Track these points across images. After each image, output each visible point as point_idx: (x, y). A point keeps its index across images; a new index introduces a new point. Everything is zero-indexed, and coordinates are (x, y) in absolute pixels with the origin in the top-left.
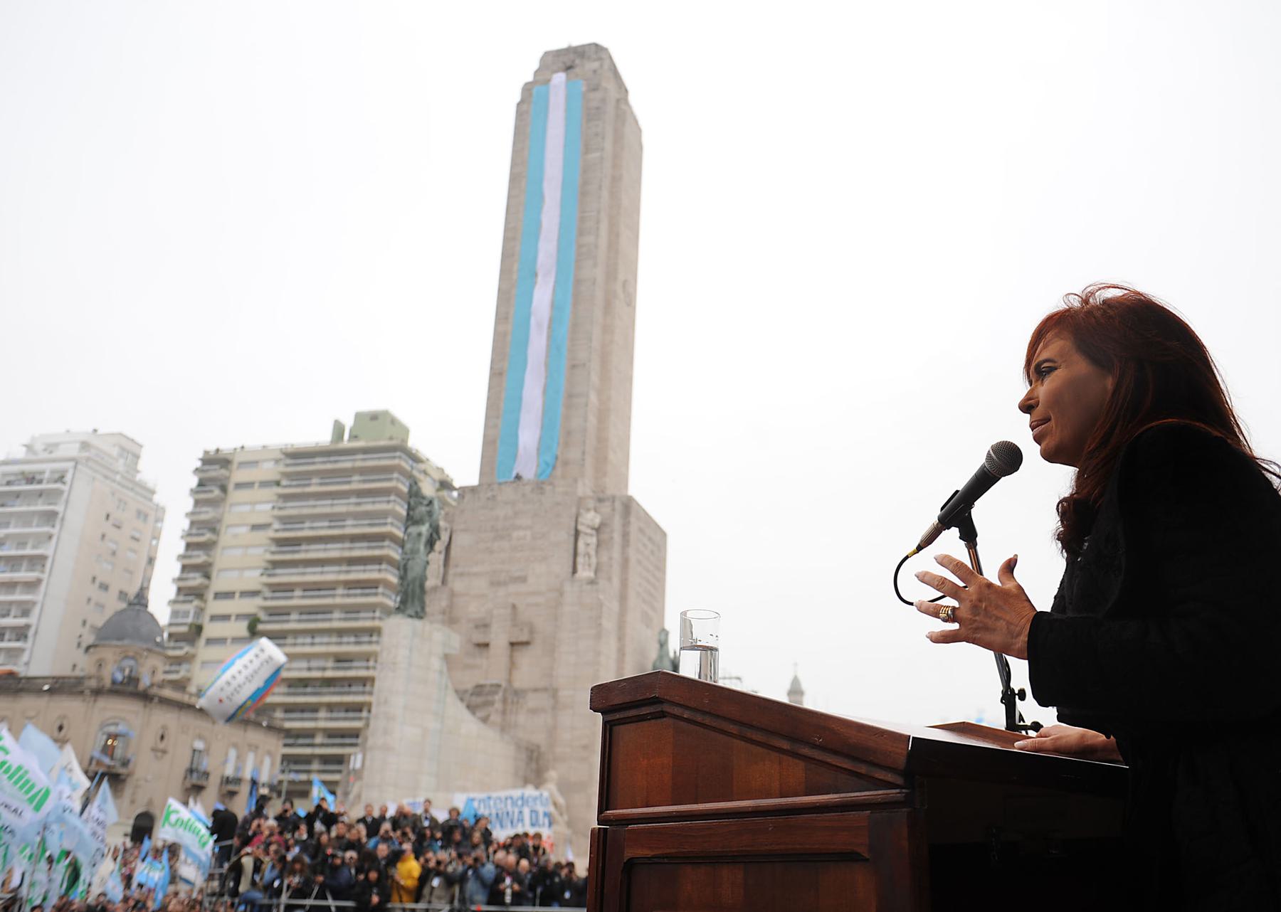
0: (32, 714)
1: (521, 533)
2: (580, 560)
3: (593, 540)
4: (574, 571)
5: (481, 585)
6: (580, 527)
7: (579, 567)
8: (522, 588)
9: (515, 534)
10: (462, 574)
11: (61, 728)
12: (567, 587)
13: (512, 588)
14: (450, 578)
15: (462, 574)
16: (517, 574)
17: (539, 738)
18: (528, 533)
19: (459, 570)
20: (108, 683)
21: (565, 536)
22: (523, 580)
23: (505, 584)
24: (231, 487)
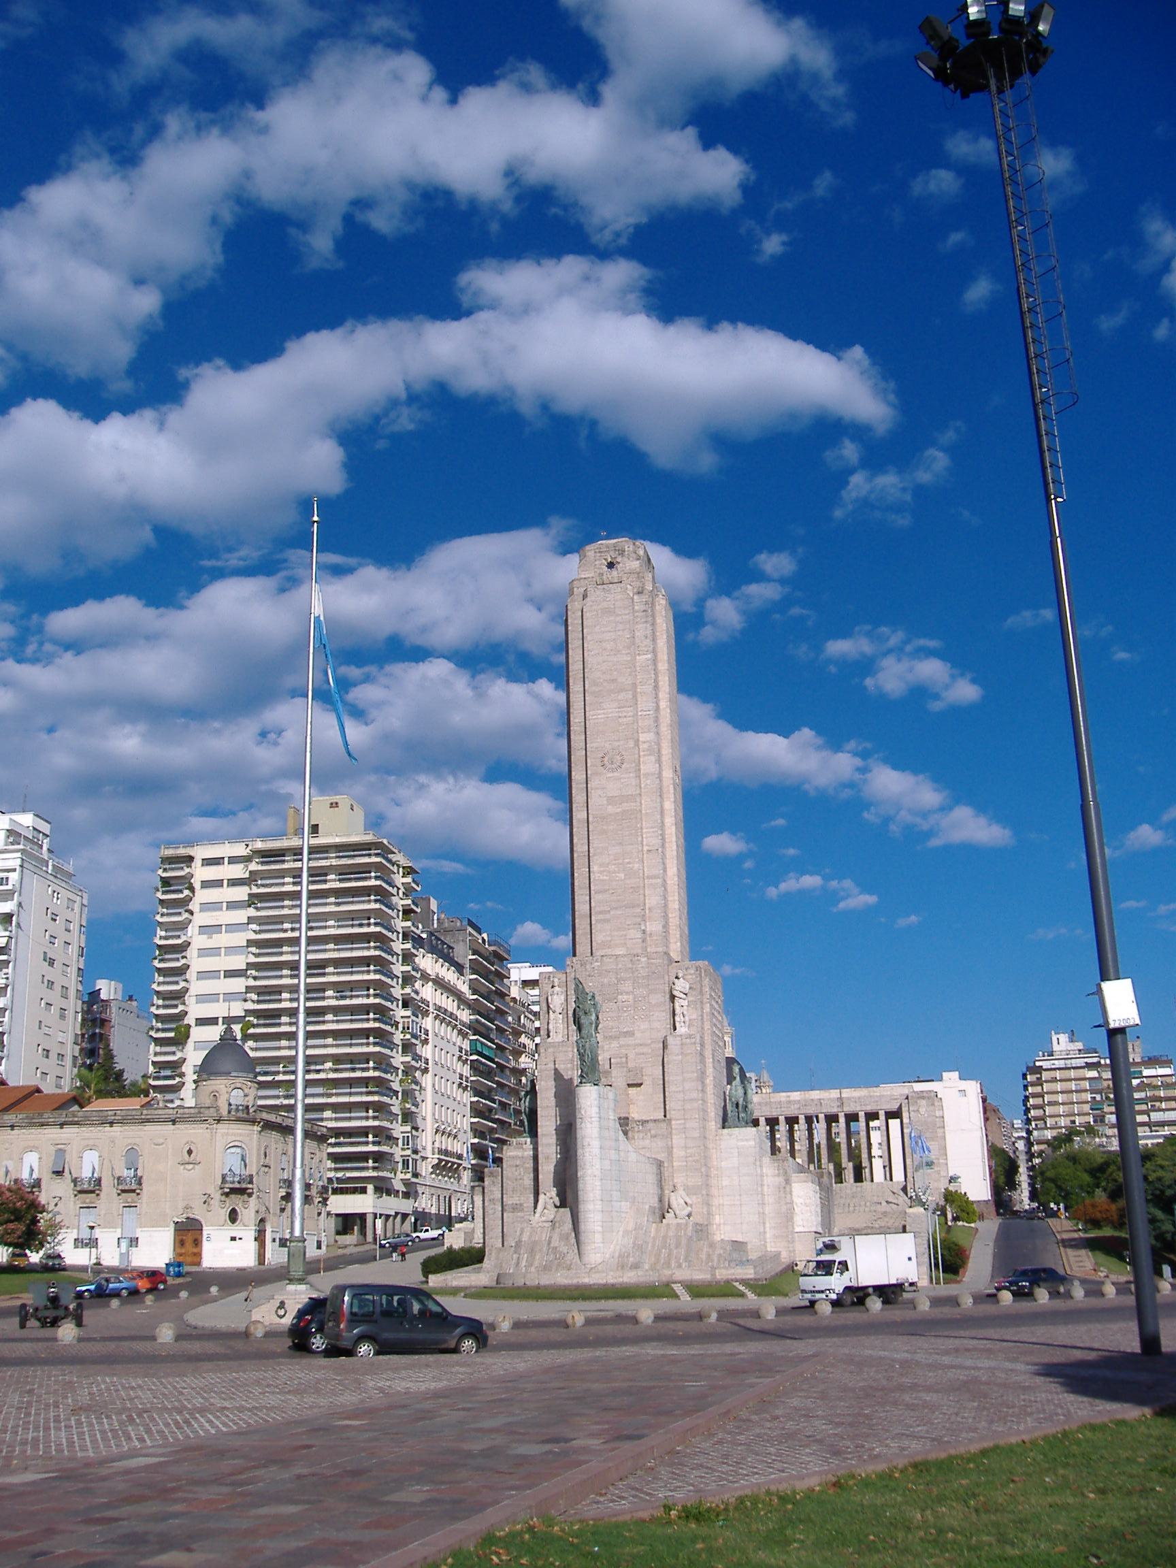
0: (161, 1141)
1: (625, 997)
2: (677, 1018)
3: (685, 1003)
4: (675, 1029)
6: (675, 993)
7: (677, 1025)
8: (630, 1041)
11: (190, 1152)
12: (670, 1040)
13: (623, 1041)
17: (661, 1156)
18: (631, 997)
20: (224, 1112)
21: (662, 998)
22: (630, 1034)
23: (617, 1038)
24: (197, 885)
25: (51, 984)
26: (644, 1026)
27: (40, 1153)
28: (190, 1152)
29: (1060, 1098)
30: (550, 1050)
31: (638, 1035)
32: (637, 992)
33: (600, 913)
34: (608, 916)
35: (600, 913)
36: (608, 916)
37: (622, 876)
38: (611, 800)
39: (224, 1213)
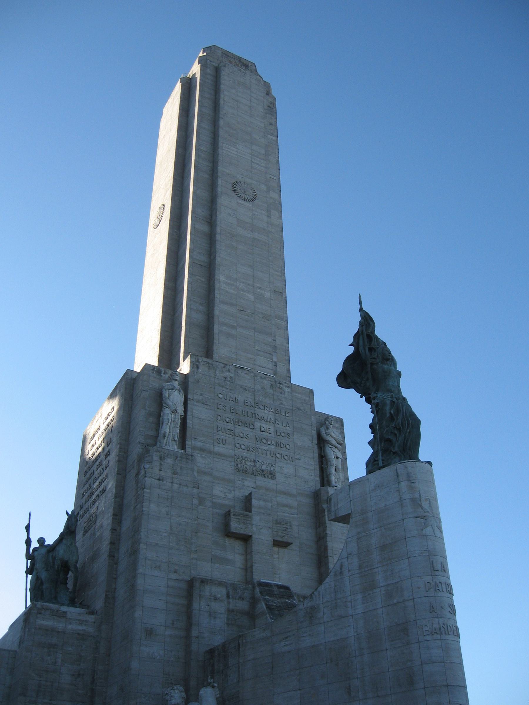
5: (226, 468)
9: (258, 424)
10: (202, 450)
13: (261, 481)
15: (202, 450)
16: (264, 467)
19: (199, 444)
22: (271, 475)
30: (170, 461)
33: (225, 325)
34: (233, 332)
35: (225, 325)
36: (233, 332)
37: (252, 297)
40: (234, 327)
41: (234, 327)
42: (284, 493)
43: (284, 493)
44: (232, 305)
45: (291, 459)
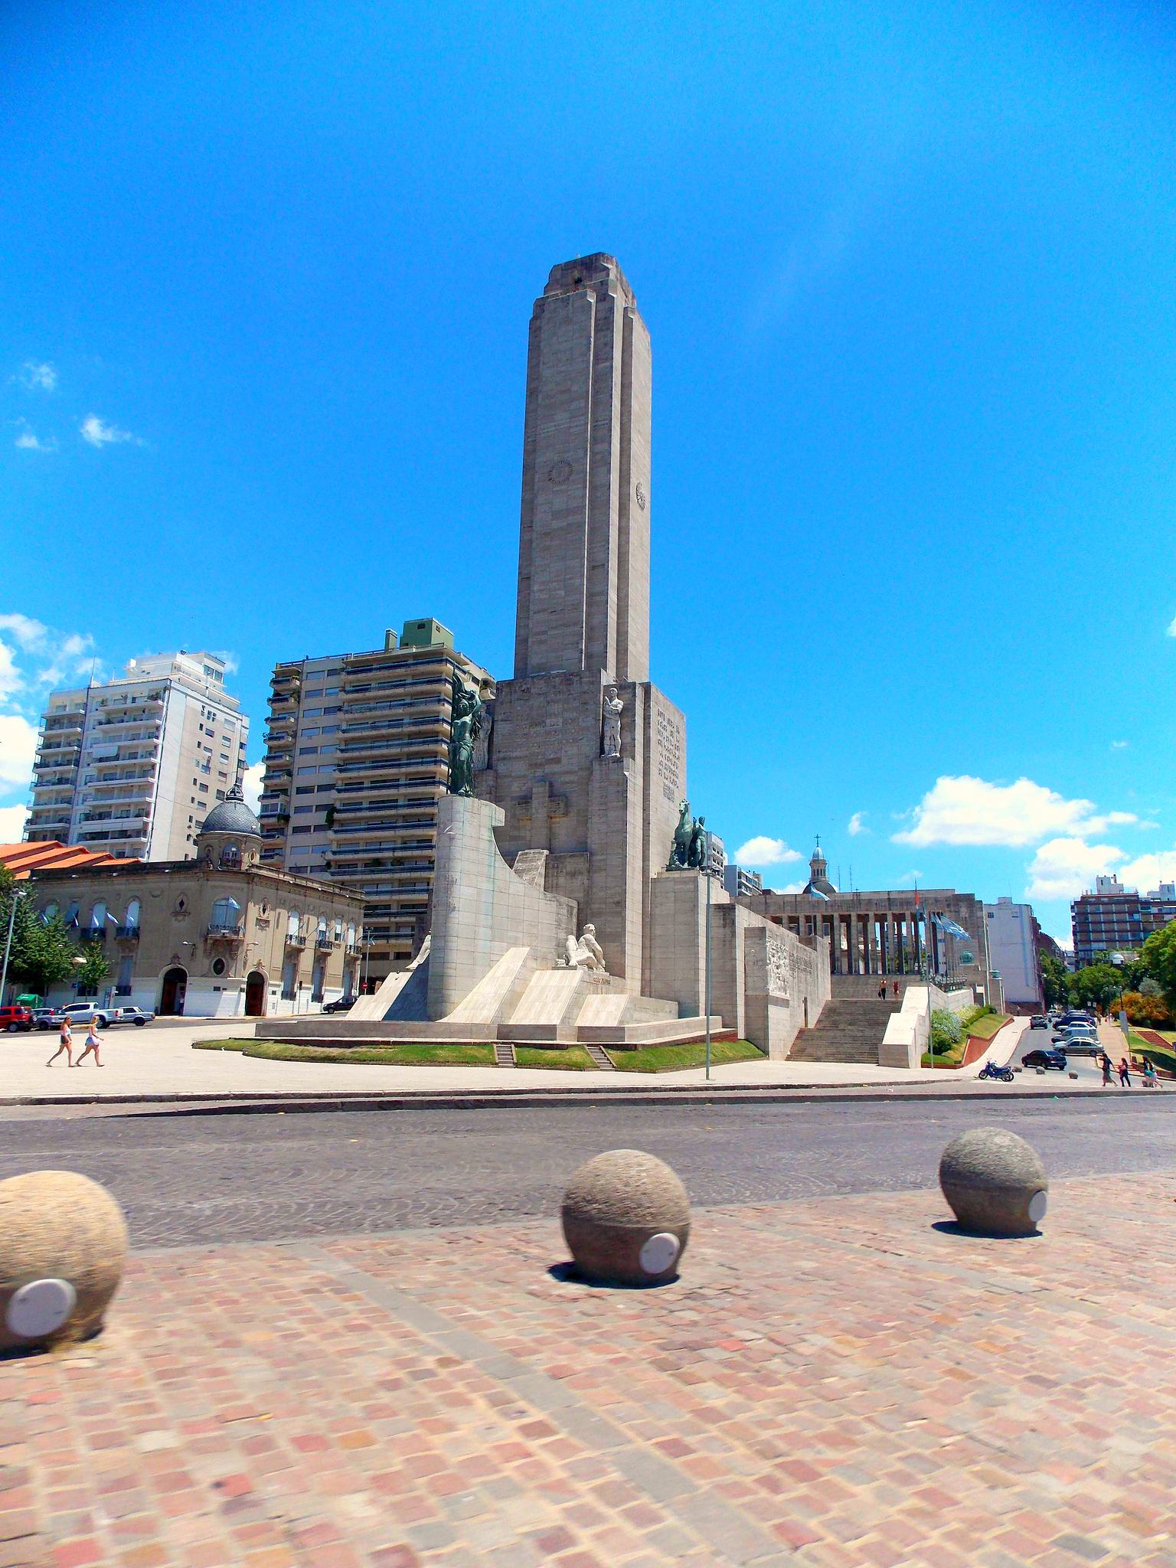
8: (556, 768)
10: (504, 759)
11: (182, 904)
13: (548, 769)
14: (494, 763)
15: (504, 759)
19: (502, 755)
22: (558, 761)
25: (204, 787)
26: (573, 750)
27: (58, 904)
28: (182, 904)
29: (1115, 917)
31: (564, 761)
32: (567, 715)
33: (538, 634)
34: (543, 637)
35: (538, 634)
36: (543, 637)
37: (562, 593)
38: (556, 515)
39: (207, 963)
40: (545, 633)
41: (545, 633)
42: (567, 773)
43: (567, 773)
44: (544, 610)
45: (575, 740)
